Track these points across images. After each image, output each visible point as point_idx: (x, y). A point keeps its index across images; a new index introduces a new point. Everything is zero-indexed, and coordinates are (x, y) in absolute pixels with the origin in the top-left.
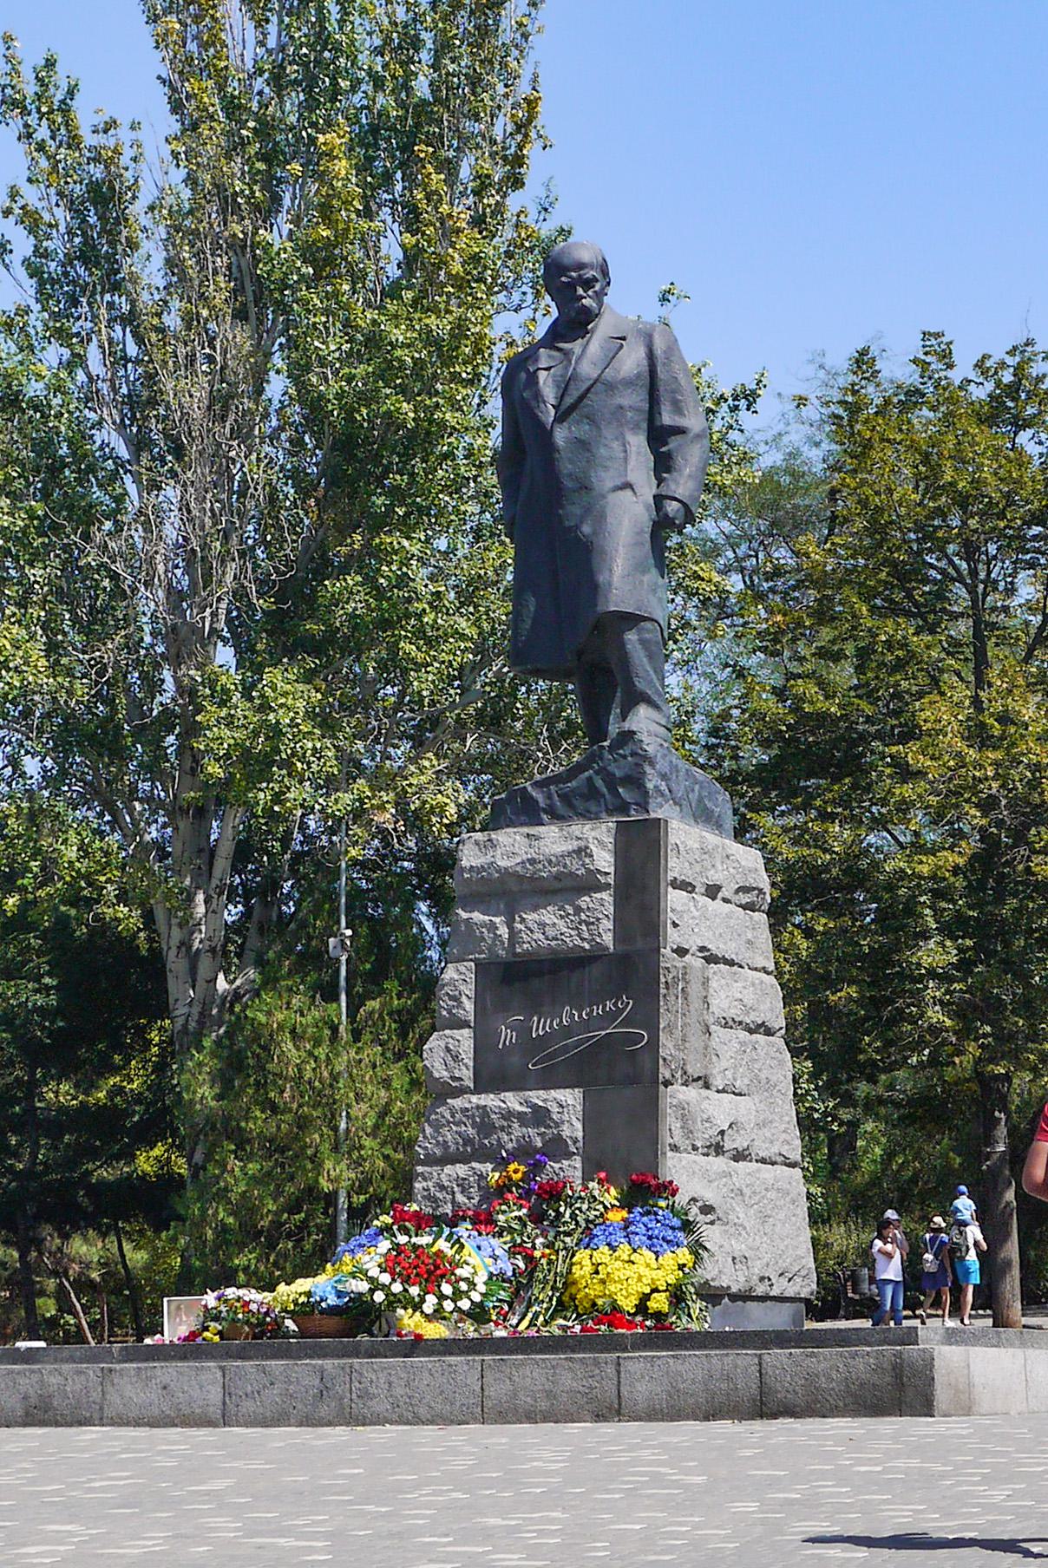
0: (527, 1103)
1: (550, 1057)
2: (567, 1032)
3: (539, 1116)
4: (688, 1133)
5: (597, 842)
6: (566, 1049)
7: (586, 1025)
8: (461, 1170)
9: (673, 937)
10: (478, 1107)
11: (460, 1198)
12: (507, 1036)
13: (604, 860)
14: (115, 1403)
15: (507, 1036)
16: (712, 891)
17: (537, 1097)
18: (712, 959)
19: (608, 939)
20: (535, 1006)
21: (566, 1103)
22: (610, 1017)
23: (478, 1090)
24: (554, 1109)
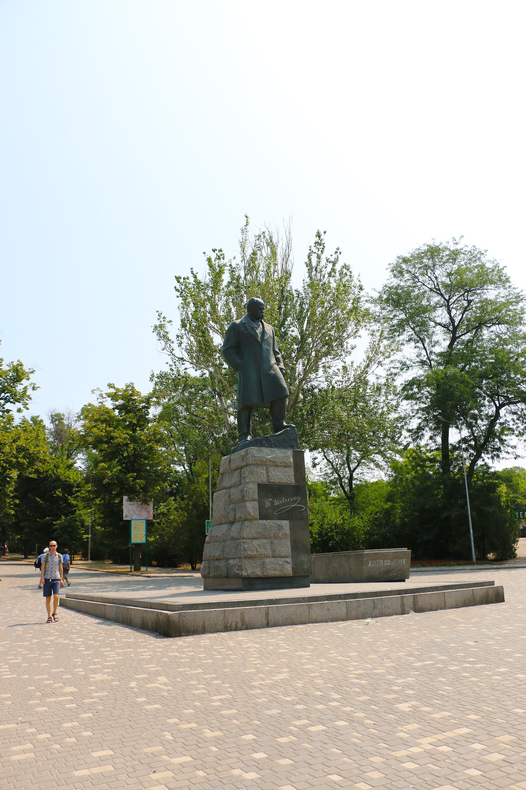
0: (276, 524)
1: (281, 511)
2: (284, 505)
3: (280, 527)
5: (287, 455)
6: (284, 509)
7: (289, 503)
10: (262, 524)
11: (259, 550)
12: (268, 504)
14: (313, 615)
15: (268, 504)
17: (278, 522)
19: (293, 480)
20: (274, 497)
21: (285, 524)
23: (260, 519)
24: (283, 525)
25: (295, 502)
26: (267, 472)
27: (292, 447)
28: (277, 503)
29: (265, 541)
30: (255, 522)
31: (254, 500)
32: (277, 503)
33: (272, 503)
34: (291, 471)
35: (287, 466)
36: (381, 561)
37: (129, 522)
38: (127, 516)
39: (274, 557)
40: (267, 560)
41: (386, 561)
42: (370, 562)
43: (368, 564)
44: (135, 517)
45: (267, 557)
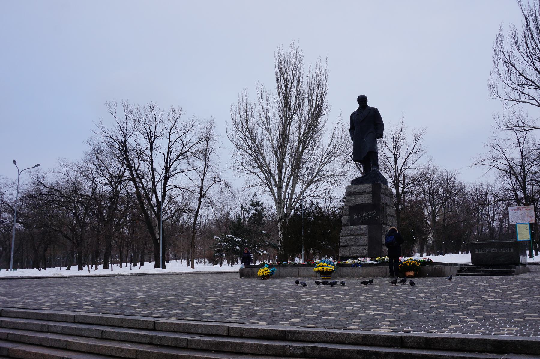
2: (365, 216)
4: (384, 232)
7: (368, 215)
8: (349, 238)
9: (382, 202)
12: (355, 217)
13: (370, 189)
15: (355, 217)
16: (386, 195)
18: (387, 205)
19: (371, 202)
21: (364, 227)
22: (372, 214)
25: (372, 214)
26: (355, 199)
27: (373, 182)
28: (361, 216)
29: (352, 237)
30: (347, 227)
31: (347, 215)
32: (361, 216)
33: (358, 216)
34: (371, 196)
35: (368, 193)
36: (487, 250)
37: (514, 226)
38: (512, 221)
39: (358, 246)
40: (354, 247)
41: (492, 250)
42: (477, 250)
43: (475, 251)
44: (519, 221)
45: (353, 246)
